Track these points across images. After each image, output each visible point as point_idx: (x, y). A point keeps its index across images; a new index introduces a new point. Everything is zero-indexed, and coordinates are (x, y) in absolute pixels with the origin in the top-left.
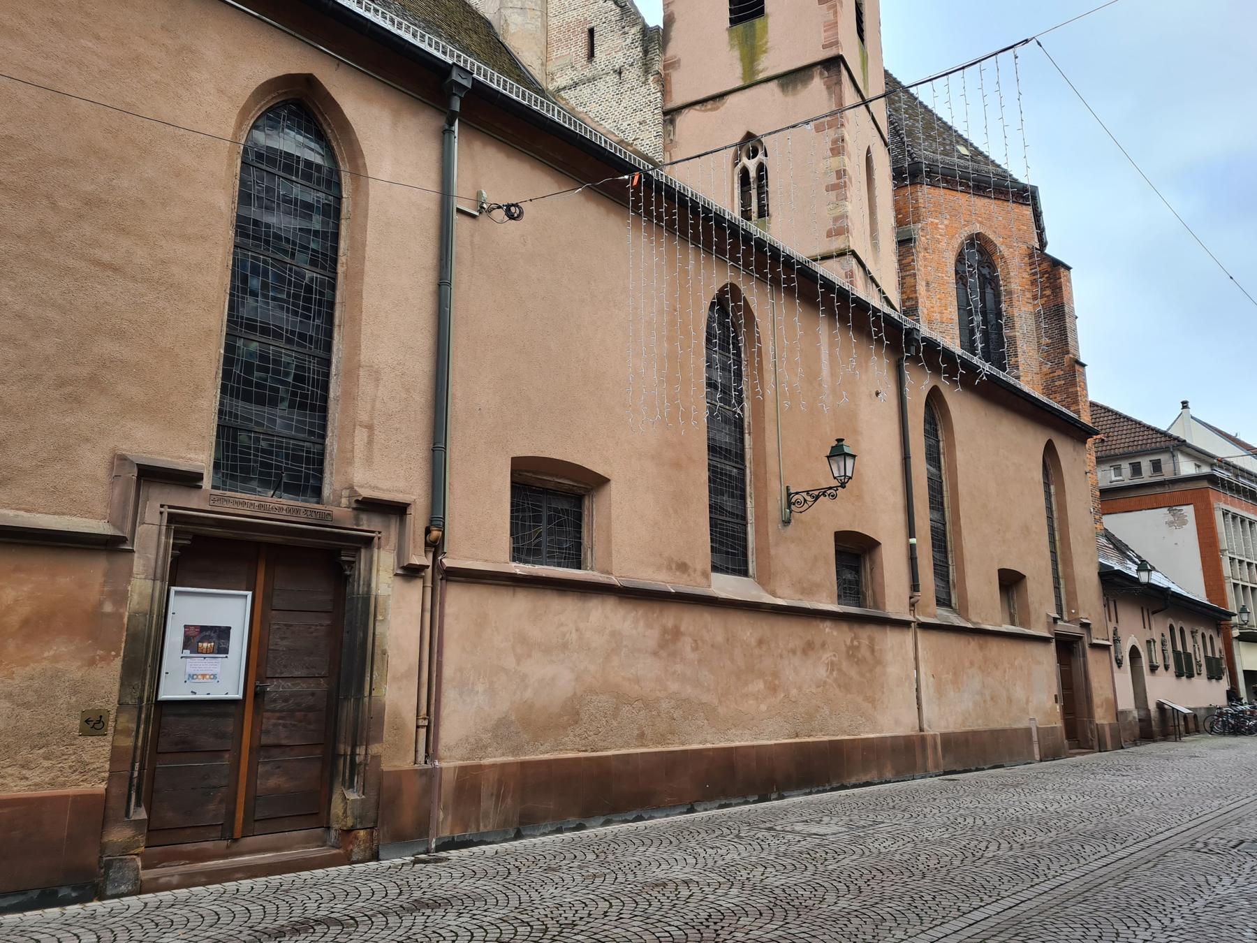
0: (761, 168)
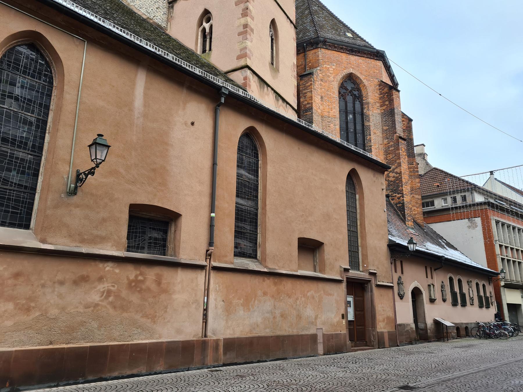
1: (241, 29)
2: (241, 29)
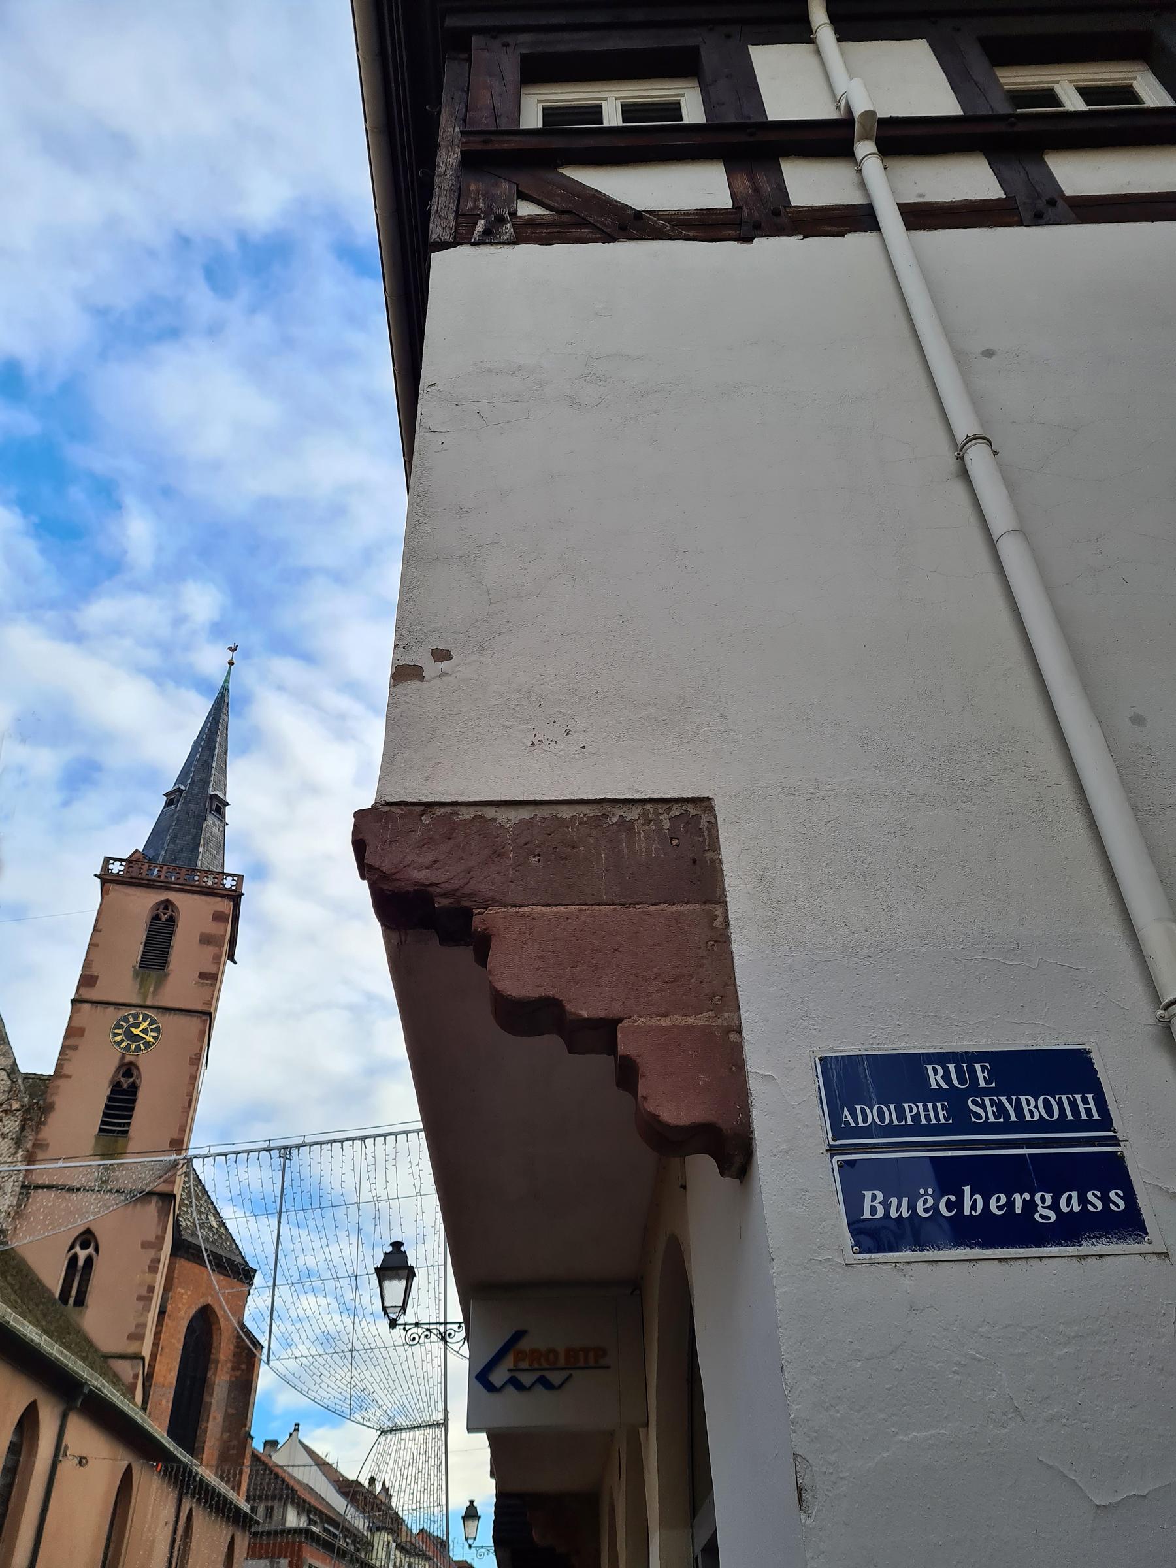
0: (89, 1261)
1: (144, 1292)
2: (144, 1292)
